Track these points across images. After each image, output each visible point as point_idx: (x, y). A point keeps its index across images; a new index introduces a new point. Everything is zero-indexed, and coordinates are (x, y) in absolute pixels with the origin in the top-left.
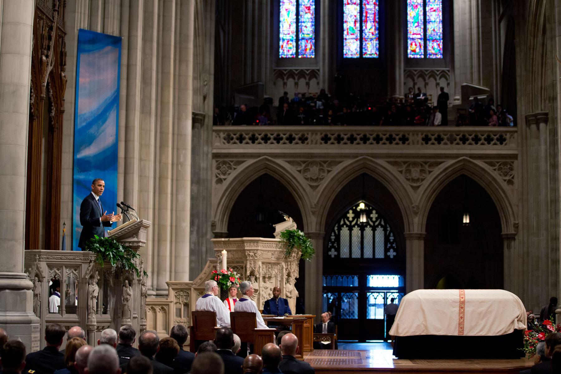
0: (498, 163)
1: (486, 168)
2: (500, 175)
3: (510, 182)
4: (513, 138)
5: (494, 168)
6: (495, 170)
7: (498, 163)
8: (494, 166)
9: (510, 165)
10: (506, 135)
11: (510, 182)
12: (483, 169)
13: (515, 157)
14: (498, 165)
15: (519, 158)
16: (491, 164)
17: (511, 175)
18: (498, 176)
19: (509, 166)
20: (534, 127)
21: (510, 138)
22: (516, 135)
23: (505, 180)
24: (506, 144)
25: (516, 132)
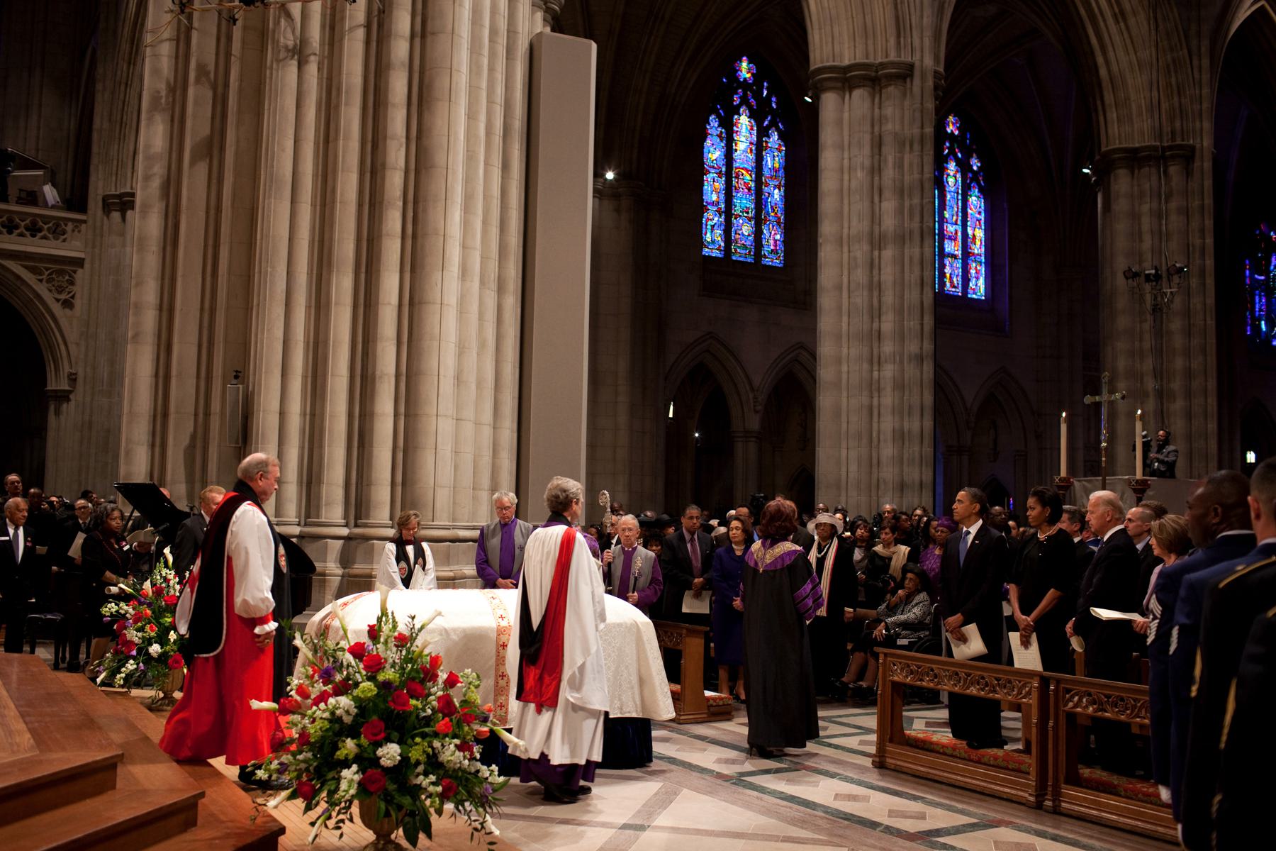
0: (47, 269)
1: (23, 276)
2: (50, 291)
3: (68, 304)
4: (79, 231)
5: (41, 277)
6: (41, 281)
7: (47, 269)
8: (41, 274)
9: (70, 276)
10: (66, 225)
11: (68, 304)
12: (18, 277)
13: (79, 263)
14: (47, 273)
15: (87, 265)
16: (34, 270)
17: (69, 293)
18: (47, 292)
19: (67, 278)
20: (116, 216)
21: (73, 231)
22: (83, 227)
23: (58, 300)
24: (64, 240)
25: (85, 222)
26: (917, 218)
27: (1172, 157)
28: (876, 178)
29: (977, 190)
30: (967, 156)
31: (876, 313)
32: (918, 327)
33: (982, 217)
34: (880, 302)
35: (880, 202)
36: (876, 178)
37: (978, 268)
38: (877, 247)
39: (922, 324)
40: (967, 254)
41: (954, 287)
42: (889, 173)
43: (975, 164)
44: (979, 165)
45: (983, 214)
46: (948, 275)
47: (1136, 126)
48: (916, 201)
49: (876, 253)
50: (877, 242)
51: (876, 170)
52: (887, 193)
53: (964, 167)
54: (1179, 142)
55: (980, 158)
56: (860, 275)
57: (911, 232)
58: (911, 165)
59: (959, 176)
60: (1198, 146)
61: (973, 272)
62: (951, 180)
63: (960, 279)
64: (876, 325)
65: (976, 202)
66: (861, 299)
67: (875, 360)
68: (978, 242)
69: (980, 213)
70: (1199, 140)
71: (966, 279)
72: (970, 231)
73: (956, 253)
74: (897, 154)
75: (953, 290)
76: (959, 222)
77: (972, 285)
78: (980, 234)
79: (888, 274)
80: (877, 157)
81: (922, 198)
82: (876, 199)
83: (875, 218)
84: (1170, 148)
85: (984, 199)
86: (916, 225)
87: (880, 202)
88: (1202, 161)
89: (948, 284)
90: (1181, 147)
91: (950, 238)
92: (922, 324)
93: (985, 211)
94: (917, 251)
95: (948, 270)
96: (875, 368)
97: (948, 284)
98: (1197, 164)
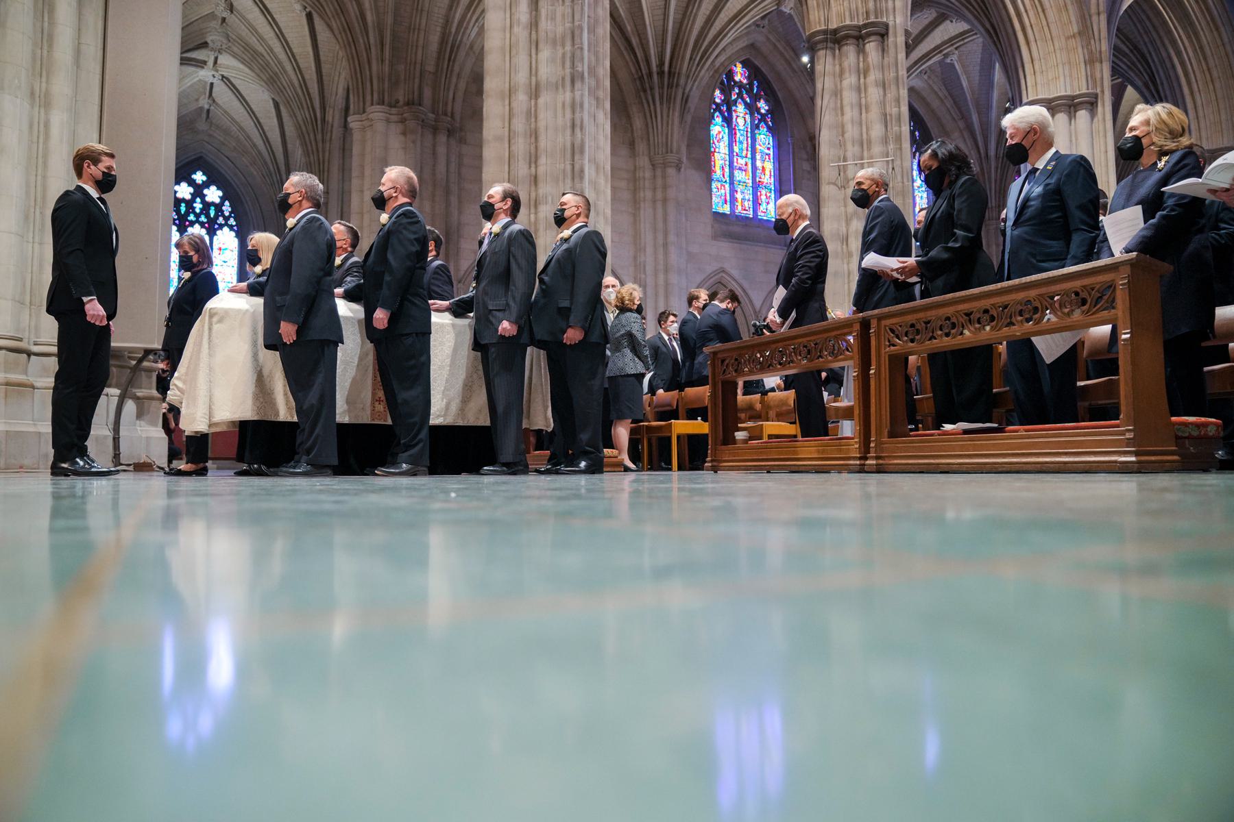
26: (568, 64)
27: (869, 35)
28: (533, 32)
29: (765, 129)
30: (756, 98)
31: (533, 159)
32: (569, 168)
33: (771, 152)
34: (536, 147)
35: (537, 54)
36: (533, 32)
37: (768, 195)
38: (533, 97)
39: (573, 165)
40: (756, 186)
41: (745, 210)
42: (544, 24)
43: (763, 106)
44: (767, 108)
45: (772, 150)
46: (740, 200)
47: (834, 9)
48: (568, 48)
49: (533, 102)
50: (535, 92)
51: (534, 24)
52: (541, 46)
53: (752, 108)
54: (872, 19)
55: (767, 101)
56: (519, 125)
57: (563, 79)
58: (563, 15)
59: (748, 117)
60: (891, 23)
61: (763, 197)
62: (741, 121)
63: (751, 203)
64: (533, 169)
65: (765, 139)
66: (521, 146)
67: (532, 203)
68: (767, 172)
69: (769, 149)
70: (891, 18)
71: (756, 202)
72: (759, 164)
73: (747, 181)
74: (550, 7)
75: (745, 212)
76: (749, 156)
77: (763, 208)
78: (769, 166)
79: (545, 118)
80: (534, 13)
81: (573, 45)
82: (533, 51)
83: (533, 71)
84: (866, 26)
85: (773, 136)
86: (568, 71)
87: (537, 54)
88: (896, 37)
89: (740, 208)
90: (873, 24)
91: (740, 169)
92: (573, 165)
93: (773, 146)
94: (568, 94)
95: (739, 196)
96: (533, 210)
97: (740, 208)
98: (891, 39)
